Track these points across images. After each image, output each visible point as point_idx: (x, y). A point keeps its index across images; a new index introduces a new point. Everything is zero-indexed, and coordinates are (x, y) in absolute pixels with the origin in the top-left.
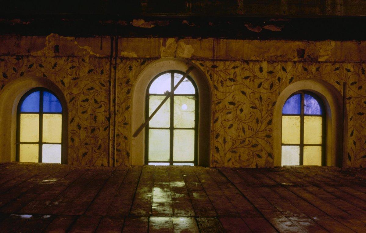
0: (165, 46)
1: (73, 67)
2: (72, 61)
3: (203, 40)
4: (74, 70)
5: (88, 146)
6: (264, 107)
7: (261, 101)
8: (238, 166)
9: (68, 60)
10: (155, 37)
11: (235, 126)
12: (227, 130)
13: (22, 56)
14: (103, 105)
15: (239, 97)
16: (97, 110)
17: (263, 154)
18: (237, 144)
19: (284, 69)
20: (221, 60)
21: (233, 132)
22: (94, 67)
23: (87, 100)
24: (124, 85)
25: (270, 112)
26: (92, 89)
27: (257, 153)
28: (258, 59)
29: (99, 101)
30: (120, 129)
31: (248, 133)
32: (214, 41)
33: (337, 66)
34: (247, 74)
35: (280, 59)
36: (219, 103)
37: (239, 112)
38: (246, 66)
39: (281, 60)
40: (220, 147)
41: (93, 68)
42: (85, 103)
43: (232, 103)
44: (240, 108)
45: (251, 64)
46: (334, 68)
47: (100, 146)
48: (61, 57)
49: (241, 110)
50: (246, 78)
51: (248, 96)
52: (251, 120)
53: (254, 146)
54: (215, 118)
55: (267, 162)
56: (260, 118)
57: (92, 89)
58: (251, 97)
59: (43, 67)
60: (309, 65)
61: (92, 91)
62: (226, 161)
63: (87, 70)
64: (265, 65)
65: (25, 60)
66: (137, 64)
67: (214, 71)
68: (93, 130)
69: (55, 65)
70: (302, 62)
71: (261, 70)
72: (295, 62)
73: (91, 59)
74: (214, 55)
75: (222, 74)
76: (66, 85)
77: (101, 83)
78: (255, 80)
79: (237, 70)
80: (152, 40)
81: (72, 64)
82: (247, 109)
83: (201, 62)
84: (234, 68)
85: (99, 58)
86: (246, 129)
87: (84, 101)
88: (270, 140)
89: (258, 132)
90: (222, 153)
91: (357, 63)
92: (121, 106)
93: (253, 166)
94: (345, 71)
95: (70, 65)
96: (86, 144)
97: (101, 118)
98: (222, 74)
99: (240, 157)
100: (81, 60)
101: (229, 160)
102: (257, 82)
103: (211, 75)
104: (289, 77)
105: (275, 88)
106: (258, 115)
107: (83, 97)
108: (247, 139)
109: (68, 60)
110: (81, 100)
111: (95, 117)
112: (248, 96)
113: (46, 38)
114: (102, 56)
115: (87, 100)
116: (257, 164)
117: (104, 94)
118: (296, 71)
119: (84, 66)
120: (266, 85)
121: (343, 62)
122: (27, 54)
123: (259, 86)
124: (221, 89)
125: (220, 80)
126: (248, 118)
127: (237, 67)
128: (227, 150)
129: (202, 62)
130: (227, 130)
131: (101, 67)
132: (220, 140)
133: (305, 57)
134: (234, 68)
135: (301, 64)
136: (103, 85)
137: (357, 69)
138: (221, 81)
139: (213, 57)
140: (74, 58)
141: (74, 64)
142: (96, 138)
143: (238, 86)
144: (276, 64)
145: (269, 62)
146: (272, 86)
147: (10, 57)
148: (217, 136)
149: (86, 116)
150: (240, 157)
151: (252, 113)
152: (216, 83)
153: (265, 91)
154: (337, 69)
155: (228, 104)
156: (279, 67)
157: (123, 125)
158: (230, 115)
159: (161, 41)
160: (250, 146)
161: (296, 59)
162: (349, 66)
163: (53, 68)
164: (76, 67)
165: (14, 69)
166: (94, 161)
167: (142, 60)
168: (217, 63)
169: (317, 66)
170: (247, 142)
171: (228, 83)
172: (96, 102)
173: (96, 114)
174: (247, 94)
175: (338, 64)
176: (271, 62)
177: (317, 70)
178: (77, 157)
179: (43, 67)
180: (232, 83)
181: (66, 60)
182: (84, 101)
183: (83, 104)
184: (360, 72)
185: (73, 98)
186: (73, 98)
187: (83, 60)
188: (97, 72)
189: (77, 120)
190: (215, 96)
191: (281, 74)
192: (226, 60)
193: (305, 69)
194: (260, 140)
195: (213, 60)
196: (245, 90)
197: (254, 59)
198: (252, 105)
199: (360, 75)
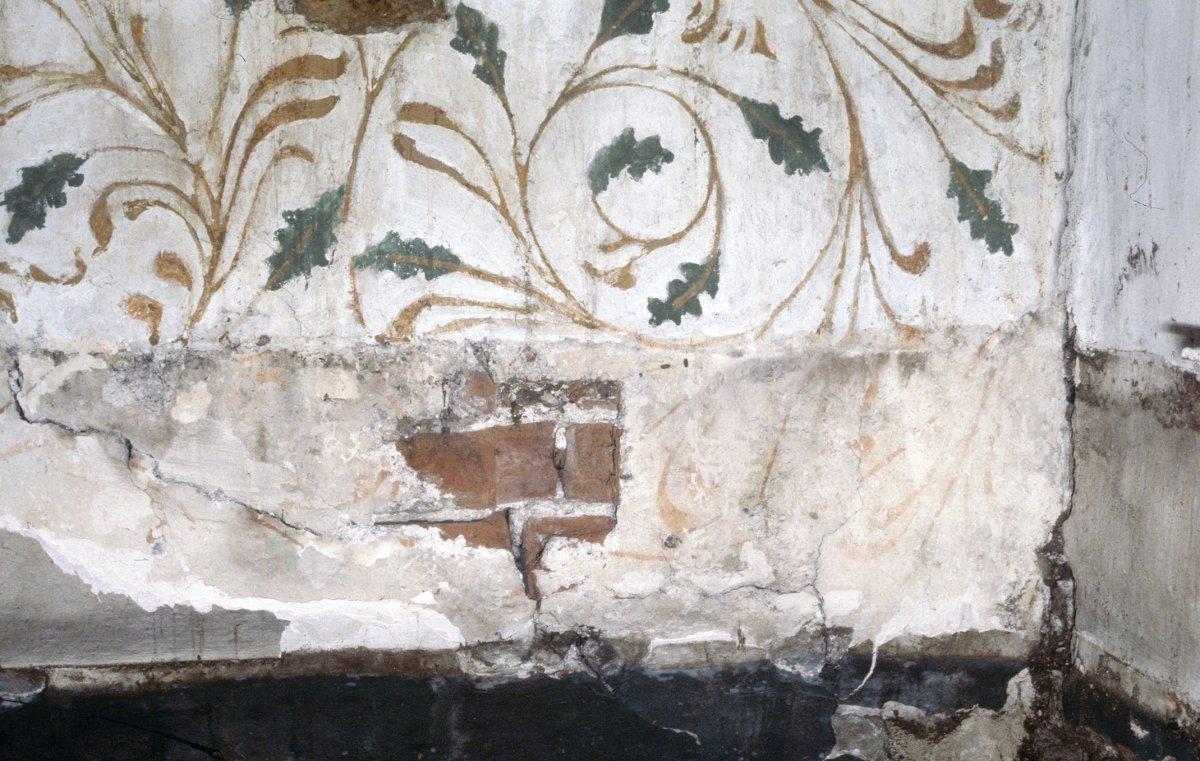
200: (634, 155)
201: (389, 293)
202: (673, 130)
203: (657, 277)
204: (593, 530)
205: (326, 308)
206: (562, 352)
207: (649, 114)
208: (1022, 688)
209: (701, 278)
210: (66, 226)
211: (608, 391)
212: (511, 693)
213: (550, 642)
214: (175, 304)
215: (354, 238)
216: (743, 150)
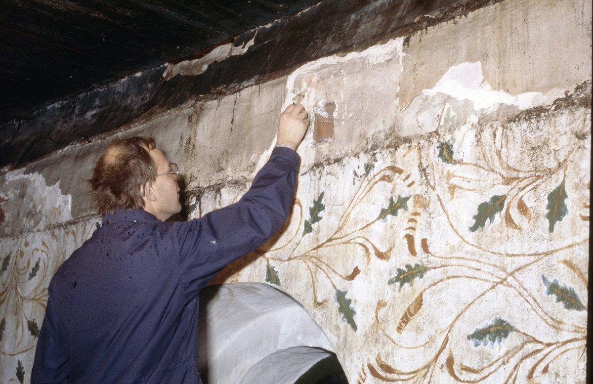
1: (394, 207)
2: (388, 173)
9: (368, 168)
22: (508, 181)
26: (500, 329)
41: (501, 190)
48: (338, 160)
57: (500, 329)
61: (497, 349)
63: (465, 209)
73: (487, 135)
76: (357, 319)
77: (554, 288)
81: (389, 186)
85: (536, 112)
95: (380, 197)
100: (433, 152)
109: (368, 168)
113: (285, 82)
114: (546, 99)
119: (453, 188)
122: (215, 179)
131: (550, 172)
140: (402, 150)
141: (402, 189)
164: (410, 203)
181: (361, 171)
188: (522, 208)
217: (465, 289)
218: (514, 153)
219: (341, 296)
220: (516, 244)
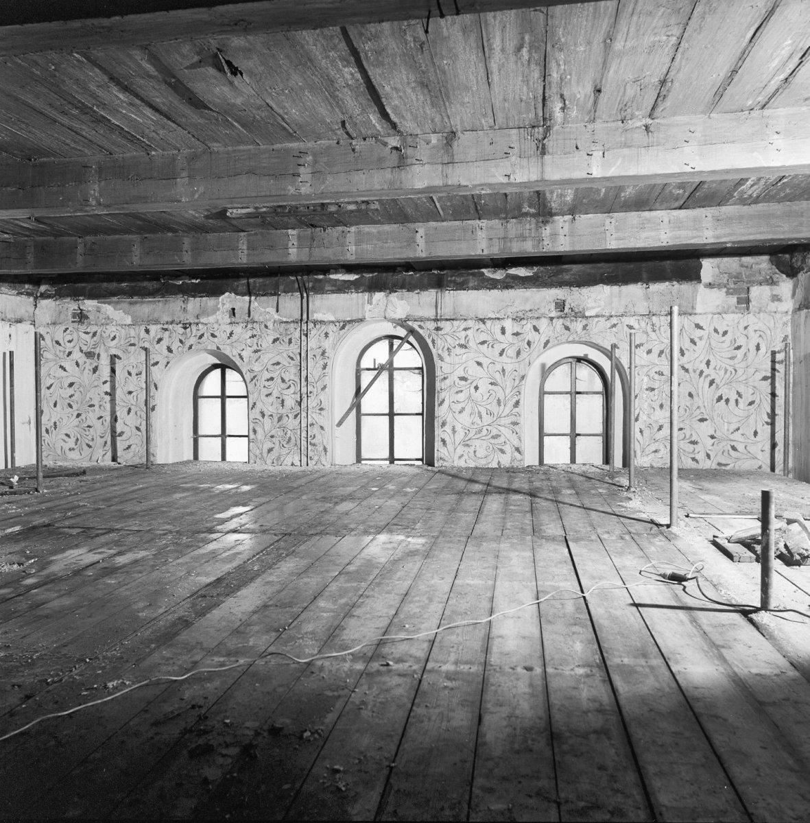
0: (371, 304)
1: (253, 336)
3: (422, 292)
4: (255, 340)
5: (274, 439)
6: (508, 383)
7: (504, 375)
8: (472, 465)
10: (358, 293)
11: (468, 410)
12: (456, 415)
13: (190, 324)
14: (292, 385)
15: (474, 371)
16: (285, 392)
17: (507, 448)
18: (471, 435)
19: (536, 329)
20: (447, 320)
21: (465, 419)
23: (272, 379)
24: (318, 357)
25: (516, 390)
26: (278, 363)
27: (500, 447)
28: (498, 316)
29: (287, 380)
30: (314, 415)
31: (487, 419)
32: (437, 293)
33: (614, 320)
34: (483, 337)
35: (530, 314)
36: (445, 378)
37: (473, 390)
38: (481, 326)
39: (531, 315)
40: (447, 439)
42: (270, 382)
43: (463, 379)
44: (474, 384)
45: (489, 323)
46: (609, 325)
47: (290, 438)
49: (476, 388)
50: (483, 343)
51: (485, 369)
52: (489, 401)
53: (496, 437)
54: (440, 400)
55: (513, 460)
56: (502, 399)
57: (278, 363)
58: (490, 369)
59: (216, 337)
60: (572, 321)
61: (278, 367)
62: (456, 458)
63: (271, 339)
64: (508, 324)
65: (194, 327)
66: (335, 329)
67: (437, 335)
68: (280, 419)
69: (231, 334)
70: (562, 318)
71: (503, 331)
72: (552, 319)
74: (437, 313)
75: (448, 338)
78: (495, 346)
79: (469, 332)
80: (354, 295)
82: (484, 386)
83: (419, 323)
84: (465, 329)
85: (287, 322)
86: (484, 414)
87: (268, 380)
88: (516, 428)
89: (500, 417)
90: (450, 446)
91: (643, 315)
92: (315, 385)
93: (495, 465)
94: (626, 329)
95: (250, 333)
96: (272, 437)
97: (290, 402)
98: (448, 338)
99: (475, 452)
100: (263, 326)
101: (460, 457)
102: (498, 348)
103: (433, 341)
104: (544, 340)
105: (523, 355)
106: (501, 395)
107: (267, 375)
108: (485, 428)
110: (263, 379)
111: (283, 401)
112: (485, 369)
115: (272, 379)
116: (499, 462)
117: (294, 370)
118: (554, 330)
120: (511, 352)
121: (622, 315)
122: (196, 321)
123: (501, 354)
124: (447, 359)
125: (446, 348)
126: (485, 398)
127: (470, 328)
128: (457, 443)
129: (422, 324)
130: (456, 415)
132: (448, 428)
133: (566, 310)
134: (465, 329)
135: (561, 321)
136: (292, 359)
137: (643, 324)
138: (448, 349)
139: (436, 316)
141: (255, 333)
142: (284, 429)
143: (471, 355)
144: (524, 322)
145: (513, 319)
146: (518, 353)
147: (175, 325)
148: (444, 424)
149: (271, 399)
150: (475, 452)
151: (491, 392)
152: (440, 352)
153: (509, 360)
154: (614, 326)
155: (457, 381)
156: (529, 326)
157: (318, 411)
158: (460, 395)
159: (366, 297)
160: (490, 436)
161: (553, 314)
162: (632, 321)
163: (229, 338)
165: (181, 341)
166: (282, 459)
167: (342, 324)
168: (440, 324)
169: (585, 322)
170: (484, 432)
171: (459, 350)
172: (283, 381)
173: (284, 397)
174: (485, 366)
175: (615, 318)
176: (517, 319)
177: (585, 327)
178: (261, 454)
179: (216, 337)
180: (464, 350)
182: (268, 380)
183: (267, 384)
184: (649, 329)
185: (254, 377)
186: (254, 377)
187: (266, 327)
189: (259, 405)
190: (439, 369)
191: (532, 336)
192: (453, 320)
193: (567, 328)
194: (503, 428)
195: (436, 320)
196: (481, 360)
197: (494, 316)
198: (490, 381)
199: (650, 333)
200: (70, 342)
201: (88, 330)
202: (67, 343)
203: (68, 332)
204: (74, 310)
205: (92, 329)
206: (76, 325)
207: (68, 344)
208: (39, 295)
209: (65, 331)
210: (112, 336)
211: (73, 322)
212: (81, 296)
213: (78, 300)
214: (104, 329)
215: (91, 335)
216: (61, 342)
217: (270, 355)
218: (281, 330)
219: (239, 355)
220: (281, 347)
